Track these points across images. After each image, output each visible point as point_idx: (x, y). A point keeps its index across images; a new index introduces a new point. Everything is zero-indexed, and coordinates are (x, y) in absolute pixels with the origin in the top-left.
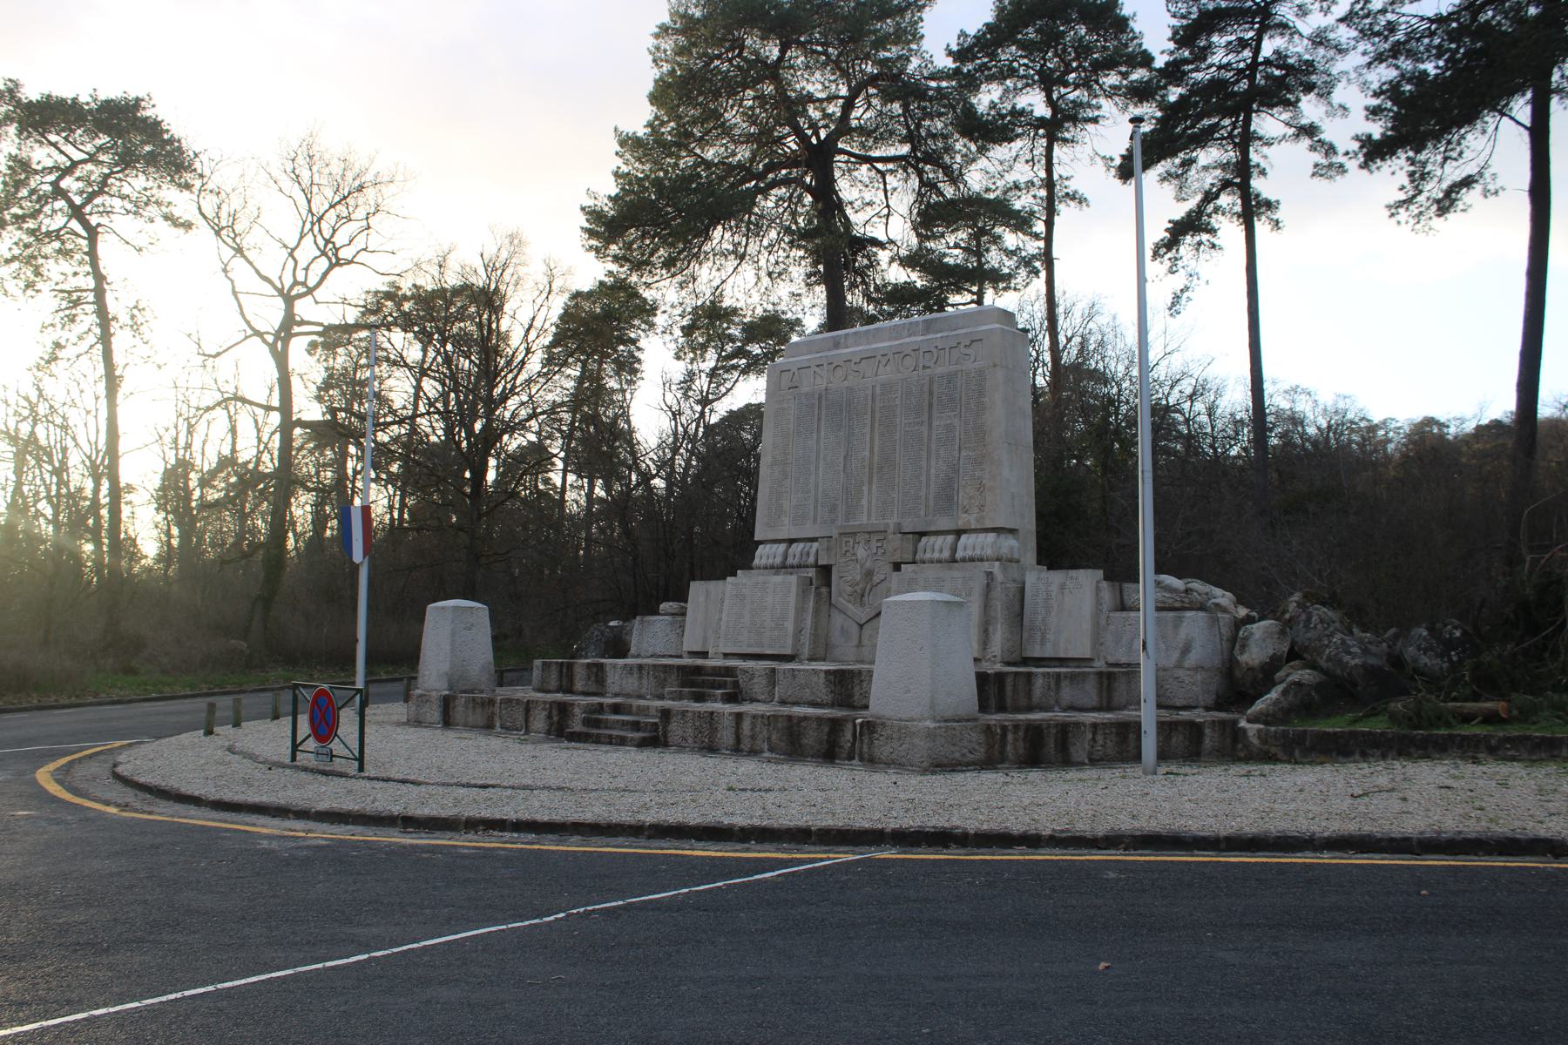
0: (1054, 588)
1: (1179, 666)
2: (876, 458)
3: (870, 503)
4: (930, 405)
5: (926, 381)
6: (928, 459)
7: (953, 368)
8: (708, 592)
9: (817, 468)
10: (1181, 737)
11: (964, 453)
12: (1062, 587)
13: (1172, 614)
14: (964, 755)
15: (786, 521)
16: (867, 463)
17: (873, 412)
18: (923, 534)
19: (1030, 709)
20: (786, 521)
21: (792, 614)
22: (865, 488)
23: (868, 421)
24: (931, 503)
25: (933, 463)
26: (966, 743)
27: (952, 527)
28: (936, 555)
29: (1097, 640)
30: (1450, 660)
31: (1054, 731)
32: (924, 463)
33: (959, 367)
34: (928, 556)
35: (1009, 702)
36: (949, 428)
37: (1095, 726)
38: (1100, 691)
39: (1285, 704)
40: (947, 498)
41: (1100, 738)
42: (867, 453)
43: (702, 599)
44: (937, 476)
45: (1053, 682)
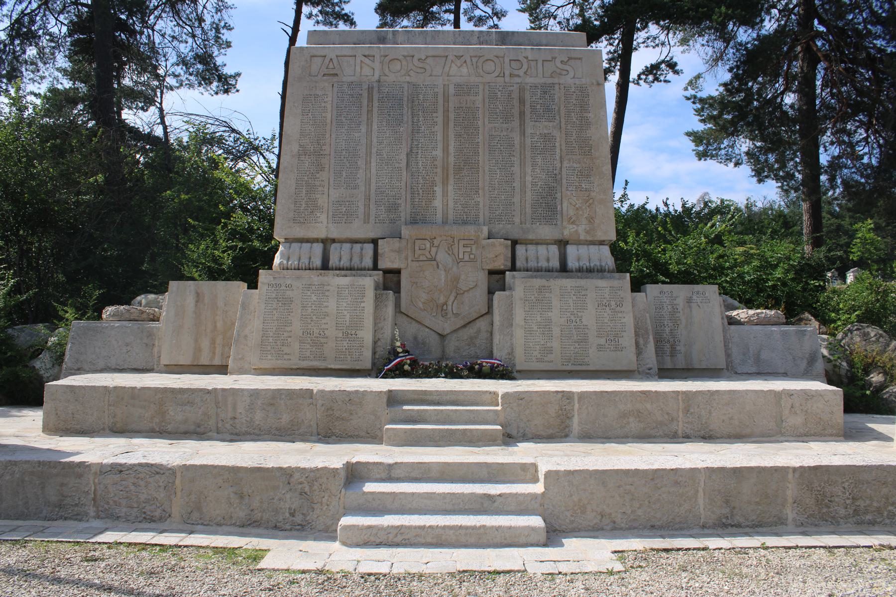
0: (680, 302)
2: (452, 159)
4: (522, 114)
6: (522, 164)
7: (550, 81)
8: (199, 297)
9: (368, 163)
11: (565, 164)
12: (689, 301)
15: (323, 217)
16: (439, 163)
17: (446, 111)
21: (368, 322)
22: (438, 190)
23: (440, 120)
24: (529, 210)
25: (529, 170)
27: (557, 236)
28: (543, 264)
32: (516, 169)
33: (556, 81)
34: (532, 264)
36: (547, 138)
40: (548, 208)
42: (439, 153)
43: (190, 300)
44: (534, 184)
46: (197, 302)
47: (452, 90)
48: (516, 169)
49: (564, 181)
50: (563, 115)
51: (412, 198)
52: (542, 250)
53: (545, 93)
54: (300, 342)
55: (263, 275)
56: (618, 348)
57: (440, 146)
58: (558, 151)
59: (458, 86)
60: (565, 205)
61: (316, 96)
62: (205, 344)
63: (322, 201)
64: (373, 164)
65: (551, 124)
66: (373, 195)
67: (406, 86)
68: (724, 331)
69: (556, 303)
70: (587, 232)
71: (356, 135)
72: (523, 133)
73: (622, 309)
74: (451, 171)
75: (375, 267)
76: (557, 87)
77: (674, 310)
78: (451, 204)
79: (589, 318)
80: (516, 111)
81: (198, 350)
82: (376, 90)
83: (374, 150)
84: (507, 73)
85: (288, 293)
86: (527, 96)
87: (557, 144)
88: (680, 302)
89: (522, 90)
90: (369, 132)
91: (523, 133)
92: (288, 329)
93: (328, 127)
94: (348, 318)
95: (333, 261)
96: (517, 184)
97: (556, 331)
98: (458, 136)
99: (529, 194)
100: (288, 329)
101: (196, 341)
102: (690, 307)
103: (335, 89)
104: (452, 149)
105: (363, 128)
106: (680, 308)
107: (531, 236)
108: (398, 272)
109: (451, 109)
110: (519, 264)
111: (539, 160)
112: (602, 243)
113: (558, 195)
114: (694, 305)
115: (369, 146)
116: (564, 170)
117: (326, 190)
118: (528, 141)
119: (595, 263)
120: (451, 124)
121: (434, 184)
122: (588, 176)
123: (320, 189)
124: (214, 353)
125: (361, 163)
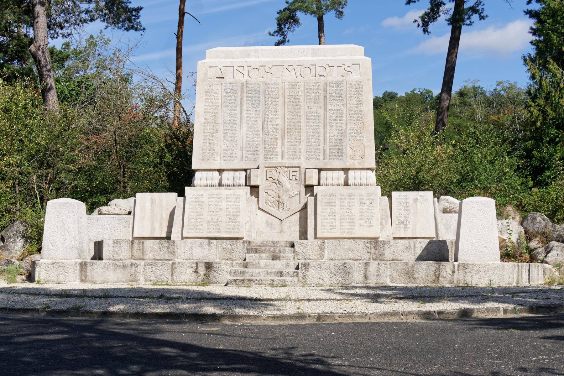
0: (411, 202)
2: (286, 125)
3: (283, 150)
4: (325, 98)
5: (322, 84)
8: (153, 202)
9: (241, 128)
11: (349, 126)
12: (416, 200)
15: (218, 158)
16: (280, 127)
18: (320, 170)
20: (218, 158)
22: (279, 142)
24: (328, 152)
25: (328, 130)
28: (335, 182)
32: (321, 130)
34: (330, 181)
36: (338, 111)
40: (338, 151)
42: (279, 121)
43: (148, 204)
46: (152, 203)
47: (286, 86)
48: (321, 130)
49: (348, 136)
50: (348, 98)
51: (265, 147)
52: (335, 173)
53: (338, 85)
54: (208, 224)
55: (188, 190)
56: (370, 225)
57: (280, 117)
58: (344, 119)
59: (289, 83)
60: (348, 148)
61: (213, 90)
62: (157, 225)
63: (217, 149)
64: (244, 129)
65: (341, 104)
66: (244, 145)
67: (261, 84)
69: (338, 202)
70: (360, 164)
71: (235, 112)
72: (325, 110)
73: (373, 205)
74: (286, 132)
75: (246, 185)
76: (345, 82)
77: (407, 205)
78: (286, 150)
79: (355, 210)
80: (322, 97)
81: (153, 229)
82: (245, 86)
83: (244, 121)
84: (317, 75)
85: (202, 199)
86: (328, 88)
87: (344, 115)
88: (411, 202)
89: (325, 84)
90: (242, 110)
91: (325, 110)
92: (202, 217)
93: (220, 108)
94: (232, 211)
95: (224, 182)
96: (322, 138)
97: (338, 217)
98: (290, 112)
99: (328, 143)
100: (202, 217)
101: (152, 224)
102: (416, 204)
103: (223, 86)
104: (286, 119)
105: (239, 109)
106: (411, 204)
107: (329, 167)
108: (257, 187)
109: (286, 97)
110: (322, 182)
111: (334, 124)
112: (369, 169)
113: (344, 144)
114: (418, 203)
115: (242, 119)
116: (348, 129)
117: (219, 143)
118: (328, 114)
119: (364, 181)
120: (286, 106)
121: (277, 139)
122: (361, 132)
123: (216, 142)
124: (162, 230)
125: (238, 128)
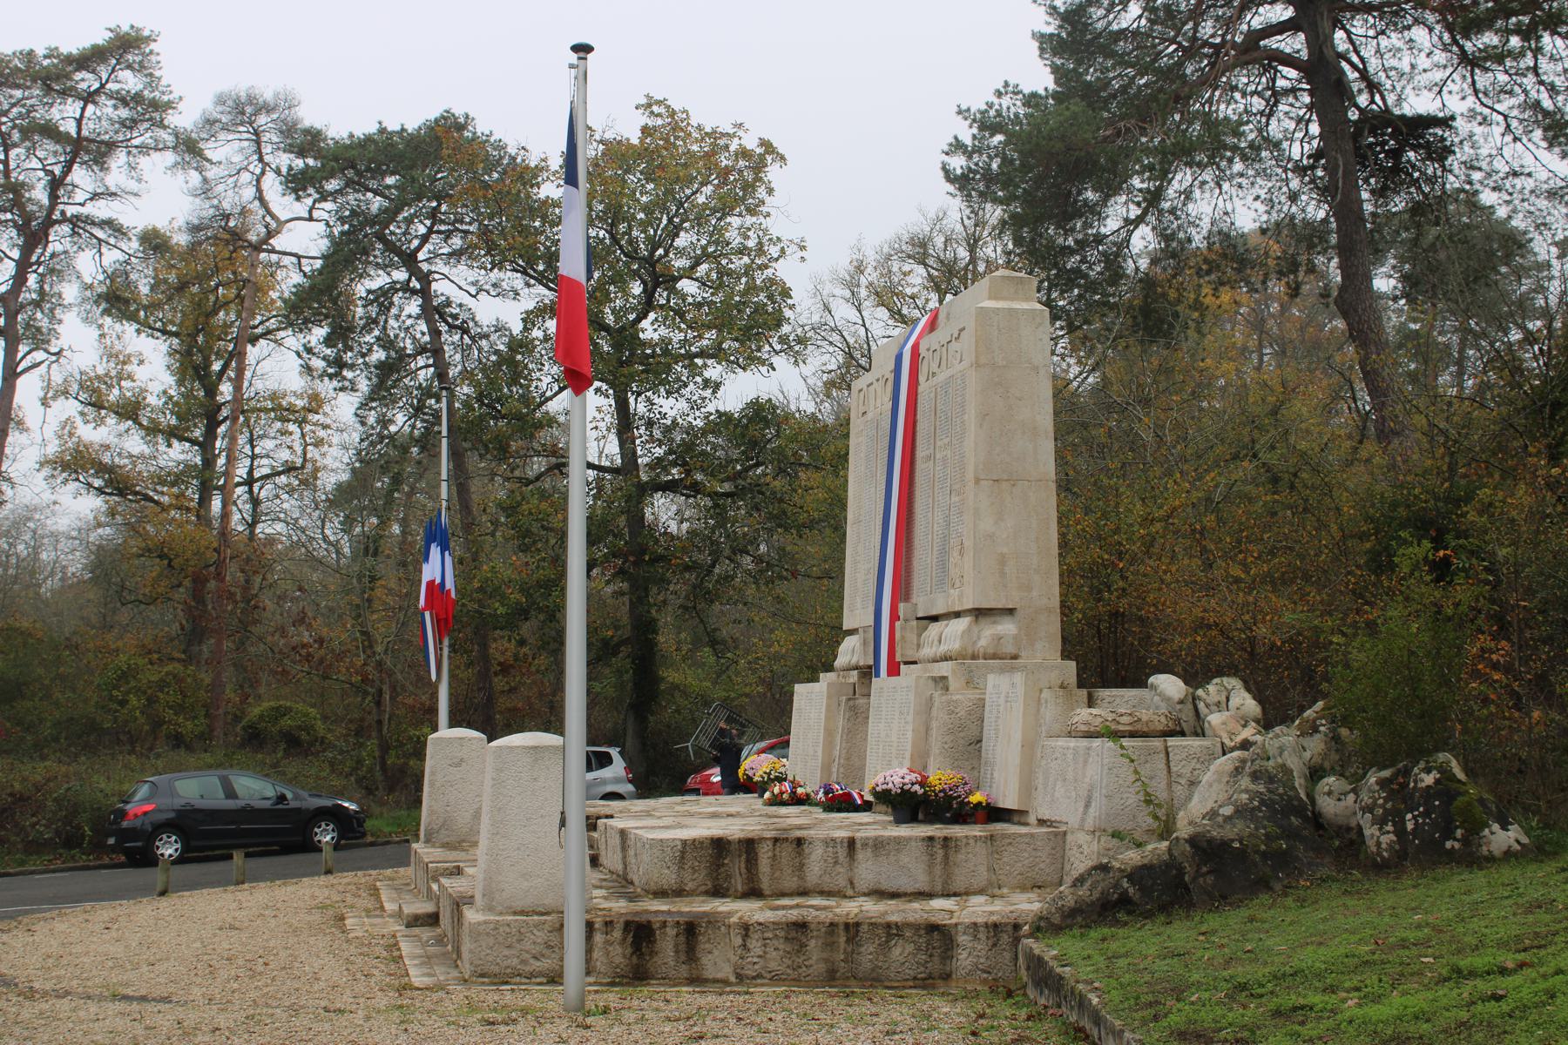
1: (1081, 828)
10: (910, 948)
13: (1084, 742)
14: (523, 962)
19: (804, 893)
26: (527, 945)
29: (1028, 787)
30: (1400, 831)
31: (671, 931)
35: (765, 884)
37: (746, 929)
38: (931, 866)
39: (1070, 902)
41: (755, 944)
45: (842, 853)
68: (1029, 748)
